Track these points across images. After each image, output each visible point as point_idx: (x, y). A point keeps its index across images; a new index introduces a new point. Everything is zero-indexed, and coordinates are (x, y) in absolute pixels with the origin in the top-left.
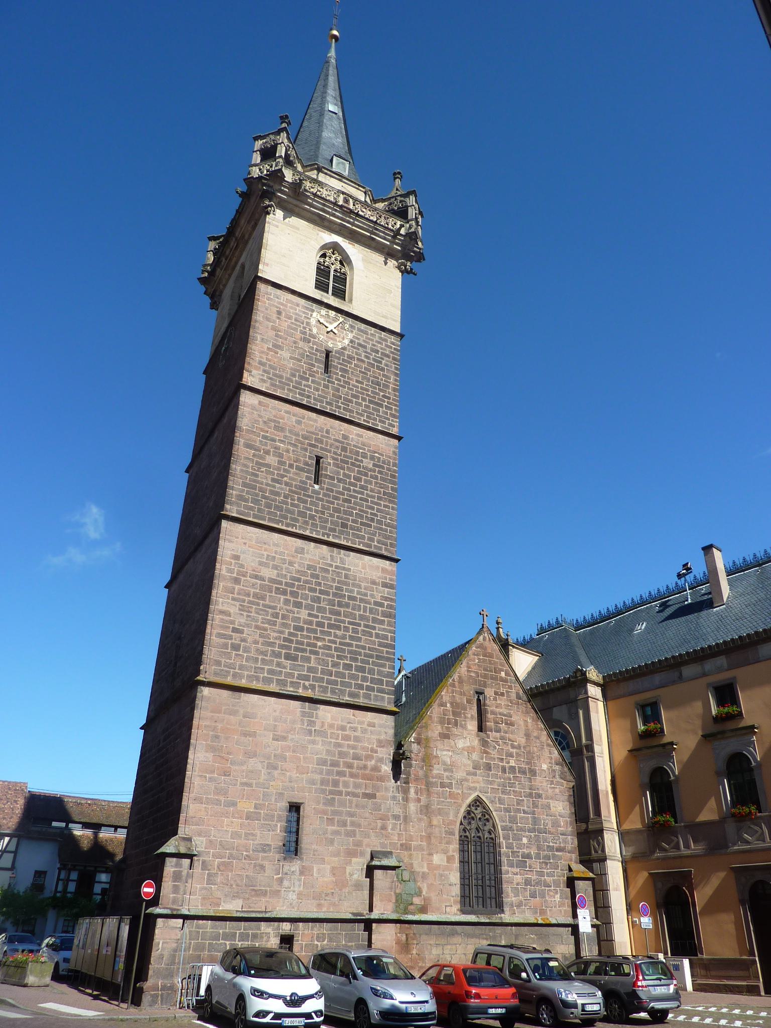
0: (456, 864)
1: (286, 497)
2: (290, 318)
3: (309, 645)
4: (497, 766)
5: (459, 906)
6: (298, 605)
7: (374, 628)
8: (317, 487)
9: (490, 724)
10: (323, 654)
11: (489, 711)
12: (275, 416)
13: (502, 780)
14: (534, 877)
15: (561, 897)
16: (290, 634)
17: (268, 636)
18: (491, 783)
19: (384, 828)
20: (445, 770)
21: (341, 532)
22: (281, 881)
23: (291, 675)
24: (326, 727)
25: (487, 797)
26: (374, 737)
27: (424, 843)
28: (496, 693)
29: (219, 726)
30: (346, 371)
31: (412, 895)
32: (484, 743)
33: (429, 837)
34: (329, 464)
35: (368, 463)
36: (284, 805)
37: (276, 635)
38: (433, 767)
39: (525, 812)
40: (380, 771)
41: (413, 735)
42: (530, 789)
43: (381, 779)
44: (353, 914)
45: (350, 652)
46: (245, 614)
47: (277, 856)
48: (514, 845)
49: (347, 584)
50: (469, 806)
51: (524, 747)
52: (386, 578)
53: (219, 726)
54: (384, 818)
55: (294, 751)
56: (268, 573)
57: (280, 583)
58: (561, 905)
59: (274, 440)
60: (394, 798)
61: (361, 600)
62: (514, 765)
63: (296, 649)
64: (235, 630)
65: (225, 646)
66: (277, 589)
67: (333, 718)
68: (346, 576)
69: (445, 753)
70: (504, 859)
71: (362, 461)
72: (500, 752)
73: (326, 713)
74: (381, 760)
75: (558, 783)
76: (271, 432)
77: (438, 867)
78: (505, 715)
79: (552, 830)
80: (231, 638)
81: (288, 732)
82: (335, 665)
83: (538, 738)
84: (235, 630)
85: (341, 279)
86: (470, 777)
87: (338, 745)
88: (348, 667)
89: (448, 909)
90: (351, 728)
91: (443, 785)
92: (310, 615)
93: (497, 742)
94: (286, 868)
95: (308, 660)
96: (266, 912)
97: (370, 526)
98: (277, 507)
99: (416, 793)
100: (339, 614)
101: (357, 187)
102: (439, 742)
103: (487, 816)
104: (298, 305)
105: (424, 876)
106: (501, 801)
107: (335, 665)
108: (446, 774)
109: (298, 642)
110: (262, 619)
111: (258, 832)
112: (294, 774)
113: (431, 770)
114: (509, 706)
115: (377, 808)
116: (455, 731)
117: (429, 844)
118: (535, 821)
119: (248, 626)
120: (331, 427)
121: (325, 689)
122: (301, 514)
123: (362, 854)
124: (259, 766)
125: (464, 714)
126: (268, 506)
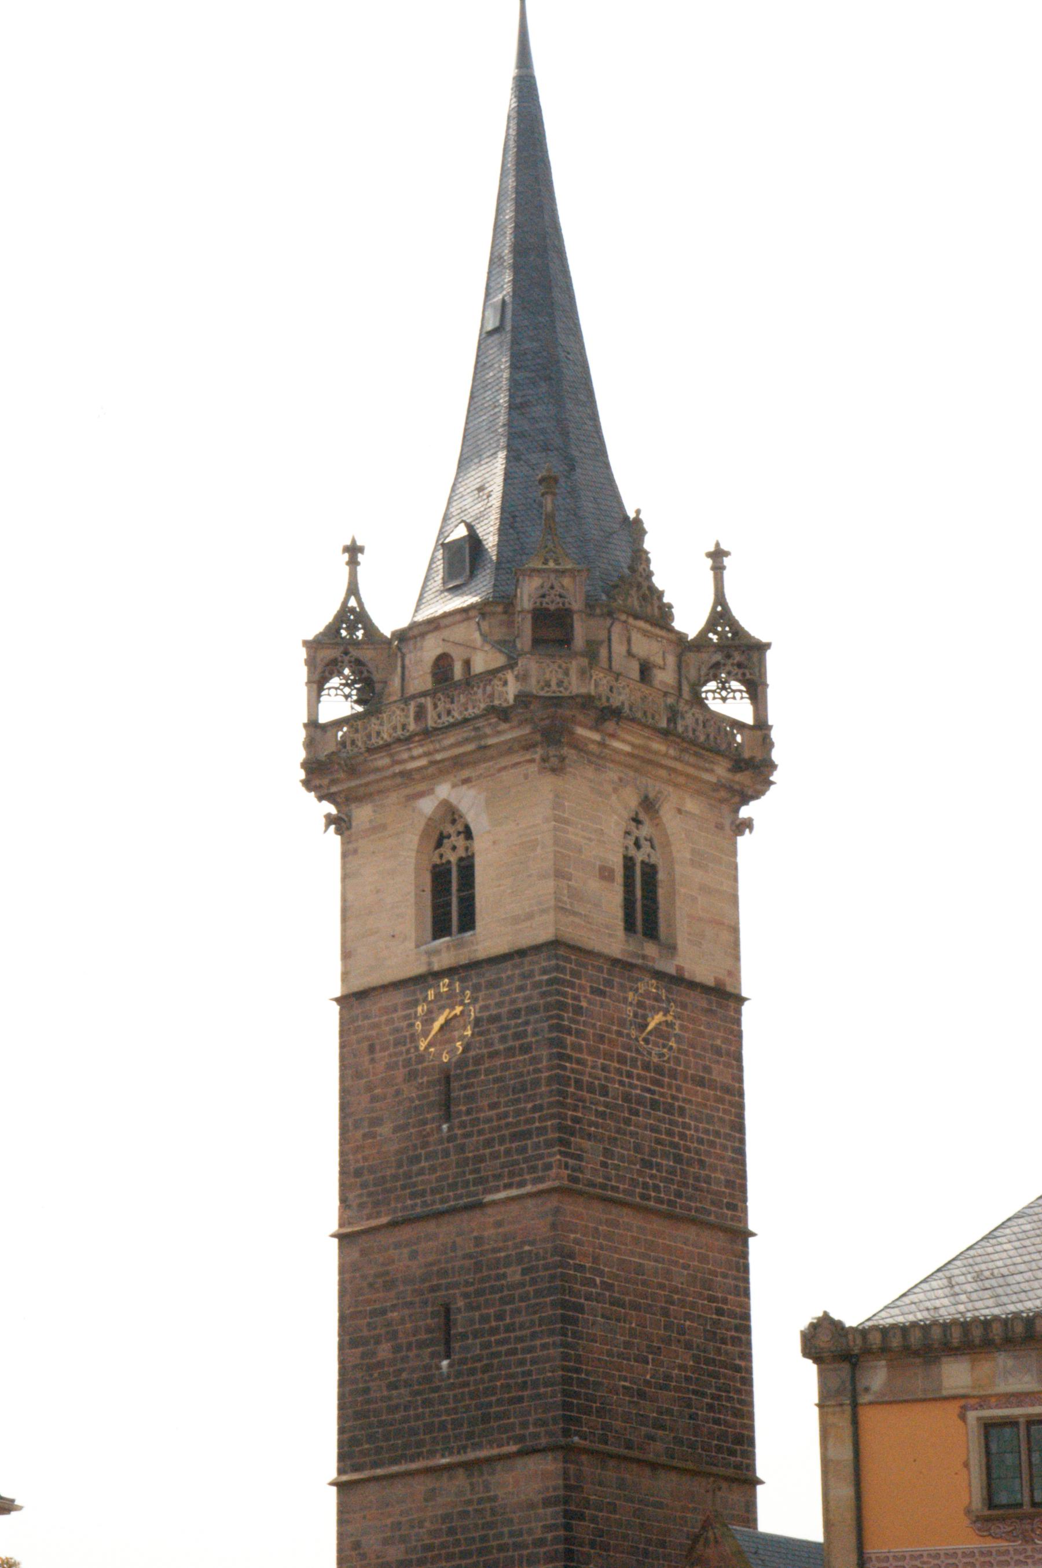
8: (445, 1363)
12: (383, 1264)
34: (459, 1310)
35: (514, 1274)
59: (383, 1312)
61: (517, 1546)
97: (520, 1400)
120: (458, 1235)
122: (429, 1428)
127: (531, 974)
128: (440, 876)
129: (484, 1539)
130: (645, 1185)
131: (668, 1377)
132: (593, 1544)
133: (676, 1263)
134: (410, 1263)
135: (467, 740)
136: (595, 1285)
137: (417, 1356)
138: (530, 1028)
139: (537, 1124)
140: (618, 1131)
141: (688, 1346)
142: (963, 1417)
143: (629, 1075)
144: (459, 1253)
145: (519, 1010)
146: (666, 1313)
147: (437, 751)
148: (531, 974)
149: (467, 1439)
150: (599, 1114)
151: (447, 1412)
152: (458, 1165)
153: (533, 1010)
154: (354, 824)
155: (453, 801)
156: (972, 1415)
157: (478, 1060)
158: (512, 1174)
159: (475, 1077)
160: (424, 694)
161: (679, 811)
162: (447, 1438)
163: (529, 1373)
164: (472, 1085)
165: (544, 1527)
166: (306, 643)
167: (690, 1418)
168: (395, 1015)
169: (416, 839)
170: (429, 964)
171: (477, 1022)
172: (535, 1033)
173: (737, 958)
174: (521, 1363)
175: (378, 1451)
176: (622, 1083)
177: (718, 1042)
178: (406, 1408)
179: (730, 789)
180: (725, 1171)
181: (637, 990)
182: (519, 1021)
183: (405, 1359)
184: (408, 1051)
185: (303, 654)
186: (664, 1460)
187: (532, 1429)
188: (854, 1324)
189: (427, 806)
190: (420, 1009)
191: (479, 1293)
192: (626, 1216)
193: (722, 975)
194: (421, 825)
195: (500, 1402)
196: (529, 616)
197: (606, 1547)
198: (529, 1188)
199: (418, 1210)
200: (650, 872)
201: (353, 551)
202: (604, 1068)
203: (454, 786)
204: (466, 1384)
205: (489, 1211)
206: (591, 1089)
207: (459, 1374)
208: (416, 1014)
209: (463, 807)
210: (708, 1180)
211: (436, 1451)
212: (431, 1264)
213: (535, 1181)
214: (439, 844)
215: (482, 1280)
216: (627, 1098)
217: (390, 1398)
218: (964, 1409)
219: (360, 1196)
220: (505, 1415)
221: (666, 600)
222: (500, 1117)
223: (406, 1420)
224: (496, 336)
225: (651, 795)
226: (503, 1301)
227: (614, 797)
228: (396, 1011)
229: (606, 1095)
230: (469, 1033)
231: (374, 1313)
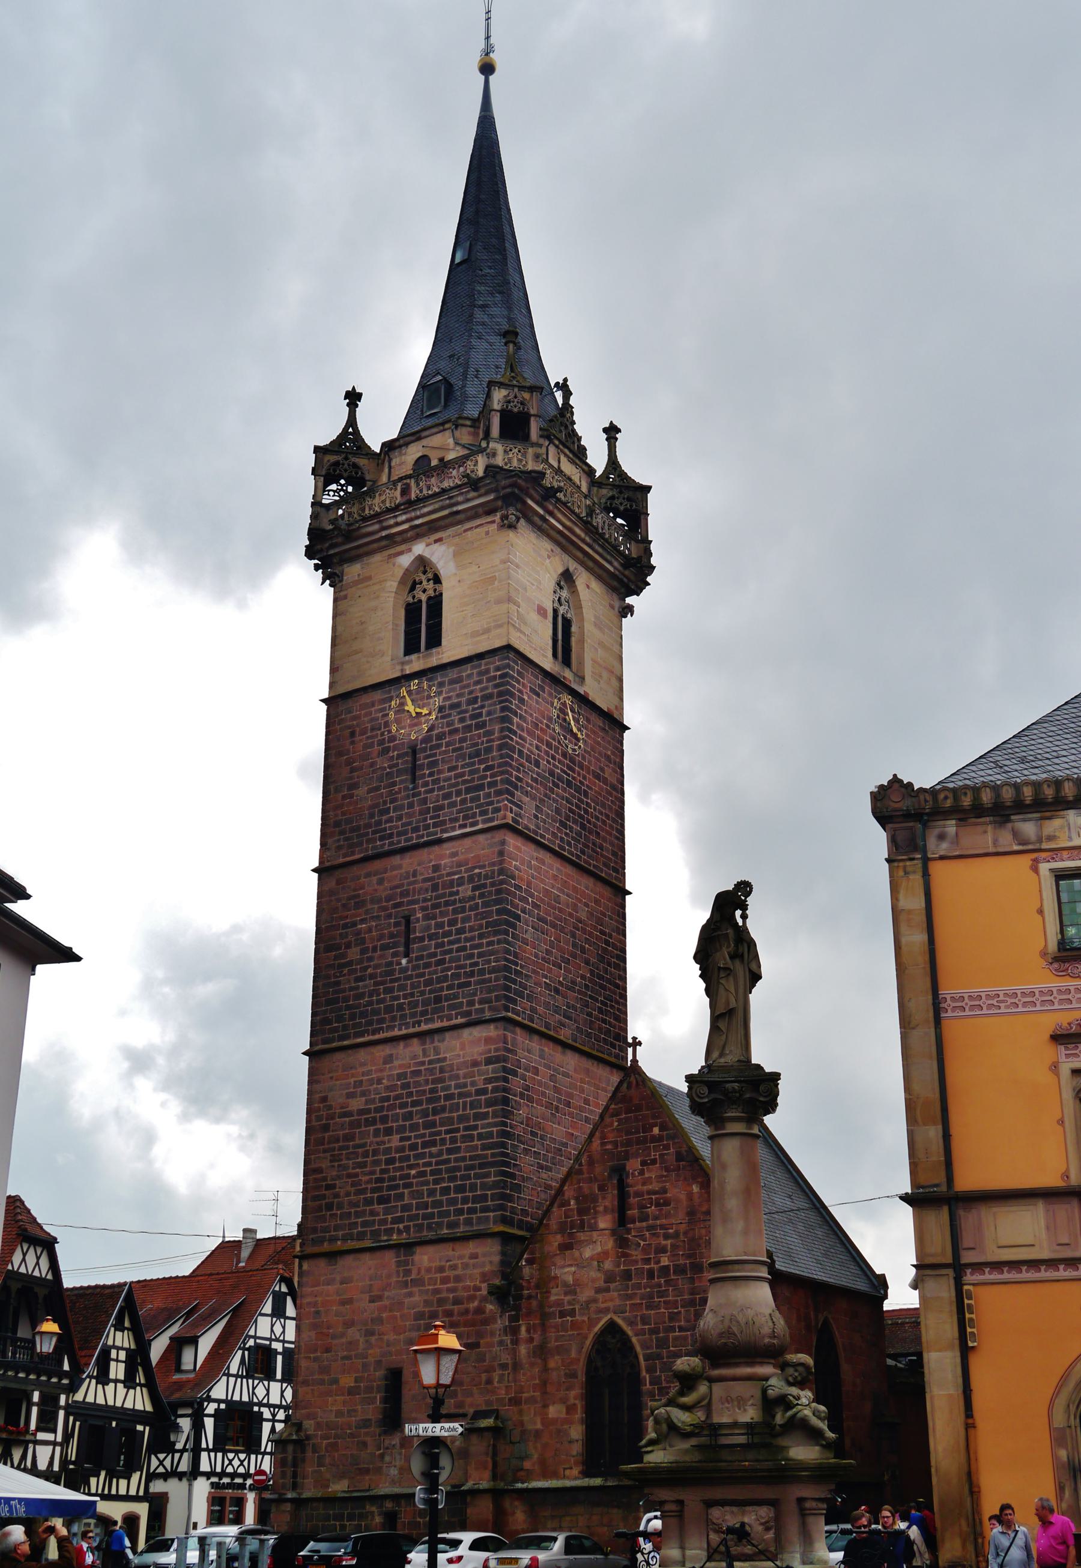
0: (579, 1415)
3: (402, 1178)
5: (580, 1468)
6: (388, 1132)
7: (475, 1127)
8: (404, 961)
10: (417, 1184)
11: (632, 1192)
13: (648, 1290)
16: (383, 1171)
17: (359, 1183)
18: (630, 1297)
19: (489, 1382)
20: (566, 1294)
21: (435, 1011)
22: (382, 1456)
23: (384, 1221)
24: (423, 1272)
25: (624, 1319)
26: (477, 1271)
28: (643, 1163)
29: (319, 1299)
32: (622, 1243)
33: (544, 1383)
34: (418, 920)
35: (466, 891)
36: (380, 1373)
37: (367, 1178)
38: (550, 1292)
39: (681, 1329)
40: (484, 1312)
41: (525, 1256)
42: (692, 1294)
43: (486, 1322)
45: (448, 1171)
46: (336, 1164)
47: (378, 1431)
48: (663, 1378)
49: (441, 1080)
51: (685, 1233)
52: (490, 1051)
53: (319, 1299)
54: (490, 1370)
55: (390, 1311)
56: (356, 1104)
57: (368, 1111)
59: (354, 924)
60: (501, 1343)
61: (460, 1095)
62: (667, 1263)
63: (390, 1188)
64: (329, 1187)
65: (320, 1209)
66: (366, 1120)
67: (430, 1260)
68: (442, 1070)
69: (566, 1270)
71: (457, 893)
72: (646, 1250)
73: (425, 1258)
77: (555, 1421)
78: (655, 1193)
80: (324, 1197)
81: (383, 1291)
82: (432, 1193)
84: (329, 1187)
85: (436, 604)
86: (600, 1296)
87: (437, 1291)
88: (445, 1191)
89: (567, 1472)
90: (450, 1266)
91: (563, 1314)
92: (402, 1139)
94: (387, 1442)
95: (400, 1197)
96: (368, 1490)
97: (469, 984)
98: (363, 1015)
99: (528, 1331)
100: (433, 1124)
101: (441, 428)
102: (559, 1257)
105: (538, 1434)
106: (645, 1320)
107: (432, 1193)
108: (568, 1298)
109: (394, 1179)
110: (353, 1163)
111: (359, 1407)
112: (392, 1337)
113: (548, 1297)
114: (663, 1176)
116: (582, 1236)
117: (544, 1393)
119: (339, 1177)
120: (419, 865)
121: (420, 1228)
122: (389, 1009)
124: (357, 1336)
125: (594, 1208)
126: (353, 1017)
127: (487, 671)
128: (412, 612)
129: (432, 1091)
130: (562, 839)
131: (573, 982)
132: (522, 1096)
133: (581, 901)
134: (376, 887)
135: (442, 508)
136: (528, 903)
137: (381, 957)
138: (484, 711)
139: (489, 780)
140: (546, 795)
141: (587, 962)
142: (1035, 869)
143: (554, 758)
144: (420, 878)
145: (477, 697)
146: (573, 936)
147: (417, 517)
148: (487, 671)
149: (422, 1016)
150: (533, 779)
151: (405, 997)
152: (421, 813)
153: (489, 697)
154: (345, 578)
155: (427, 554)
156: (1044, 868)
157: (440, 737)
158: (465, 818)
159: (438, 748)
160: (409, 477)
161: (588, 587)
162: (403, 1017)
163: (476, 964)
164: (435, 755)
165: (485, 1079)
166: (317, 450)
167: (587, 1015)
168: (373, 709)
169: (395, 584)
170: (402, 670)
171: (441, 709)
172: (489, 713)
173: (622, 699)
174: (471, 956)
175: (345, 1028)
176: (548, 762)
177: (609, 753)
178: (371, 995)
179: (620, 581)
180: (612, 844)
181: (559, 699)
182: (476, 706)
183: (370, 959)
184: (382, 734)
185: (311, 460)
186: (570, 1041)
187: (477, 1006)
188: (927, 786)
189: (405, 561)
190: (393, 703)
191: (436, 906)
192: (548, 858)
193: (613, 708)
194: (400, 573)
195: (450, 987)
196: (498, 414)
197: (530, 1099)
198: (480, 826)
199: (386, 848)
200: (567, 623)
201: (353, 398)
202: (537, 748)
203: (427, 545)
204: (423, 975)
205: (446, 845)
206: (529, 760)
207: (414, 968)
208: (390, 706)
209: (434, 559)
210: (601, 847)
211: (395, 1026)
212: (396, 887)
213: (485, 821)
214: (413, 588)
215: (437, 898)
216: (552, 773)
217: (357, 988)
218: (1036, 861)
219: (339, 840)
220: (456, 997)
221: (582, 443)
222: (457, 776)
223: (370, 1003)
224: (463, 267)
225: (571, 569)
226: (455, 911)
227: (548, 561)
228: (373, 705)
229: (538, 767)
230: (434, 717)
231: (345, 926)
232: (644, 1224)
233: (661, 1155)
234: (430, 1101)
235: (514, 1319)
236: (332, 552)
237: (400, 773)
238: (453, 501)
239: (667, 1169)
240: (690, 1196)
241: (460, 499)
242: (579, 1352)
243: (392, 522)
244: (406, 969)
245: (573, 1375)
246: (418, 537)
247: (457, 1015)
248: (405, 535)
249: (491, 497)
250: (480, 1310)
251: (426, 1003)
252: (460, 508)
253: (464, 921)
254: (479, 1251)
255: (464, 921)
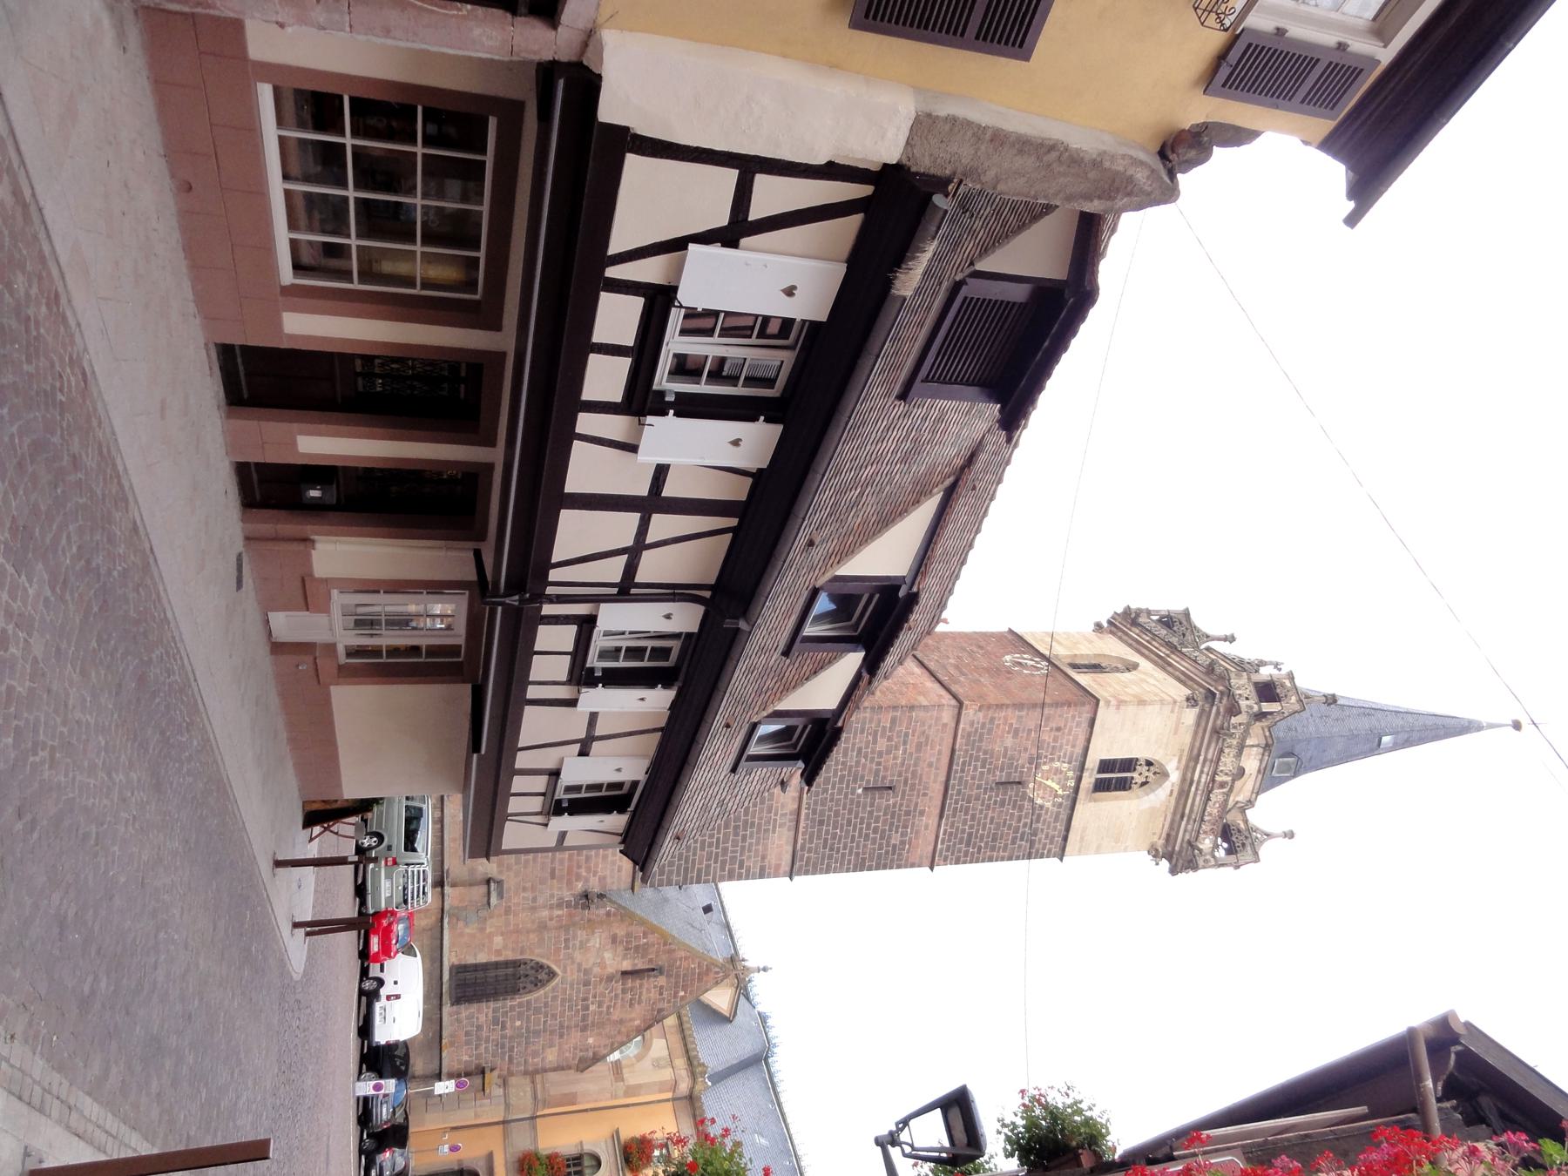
0: (494, 959)
1: (844, 763)
2: (1055, 740)
4: (588, 992)
5: (456, 963)
7: (716, 862)
8: (860, 791)
9: (629, 984)
14: (484, 1034)
15: (466, 1061)
19: (524, 889)
20: (581, 942)
21: (813, 821)
25: (557, 984)
26: (608, 873)
27: (512, 927)
28: (661, 987)
30: (1003, 804)
31: (465, 920)
32: (610, 978)
35: (896, 839)
39: (545, 1022)
40: (577, 880)
43: (569, 883)
44: (448, 871)
50: (548, 967)
51: (609, 1019)
54: (533, 889)
58: (459, 1062)
59: (905, 743)
61: (743, 848)
68: (767, 831)
70: (499, 1004)
71: (897, 832)
74: (587, 880)
75: (575, 1054)
76: (913, 740)
78: (640, 997)
79: (529, 1051)
83: (619, 1032)
85: (1123, 785)
86: (576, 966)
89: (453, 954)
91: (567, 941)
93: (611, 991)
97: (825, 847)
103: (538, 984)
104: (1073, 746)
105: (482, 930)
106: (554, 998)
115: (543, 882)
116: (620, 949)
118: (537, 1033)
123: (500, 872)
128: (1129, 764)
135: (1191, 810)
137: (870, 770)
147: (1197, 789)
184: (1046, 757)
191: (893, 814)
198: (939, 846)
232: (619, 992)
233: (664, 999)
234: (746, 822)
235: (569, 905)
236: (1215, 708)
237: (1009, 774)
238: (1191, 822)
239: (654, 1003)
240: (632, 1020)
241: (1190, 827)
242: (538, 955)
243: (1206, 770)
244: (854, 790)
245: (522, 952)
246: (1183, 780)
247: (805, 840)
248: (1191, 770)
249: (1177, 848)
250: (578, 877)
251: (822, 812)
252: (1184, 823)
253: (874, 840)
254: (624, 873)
255: (874, 840)
